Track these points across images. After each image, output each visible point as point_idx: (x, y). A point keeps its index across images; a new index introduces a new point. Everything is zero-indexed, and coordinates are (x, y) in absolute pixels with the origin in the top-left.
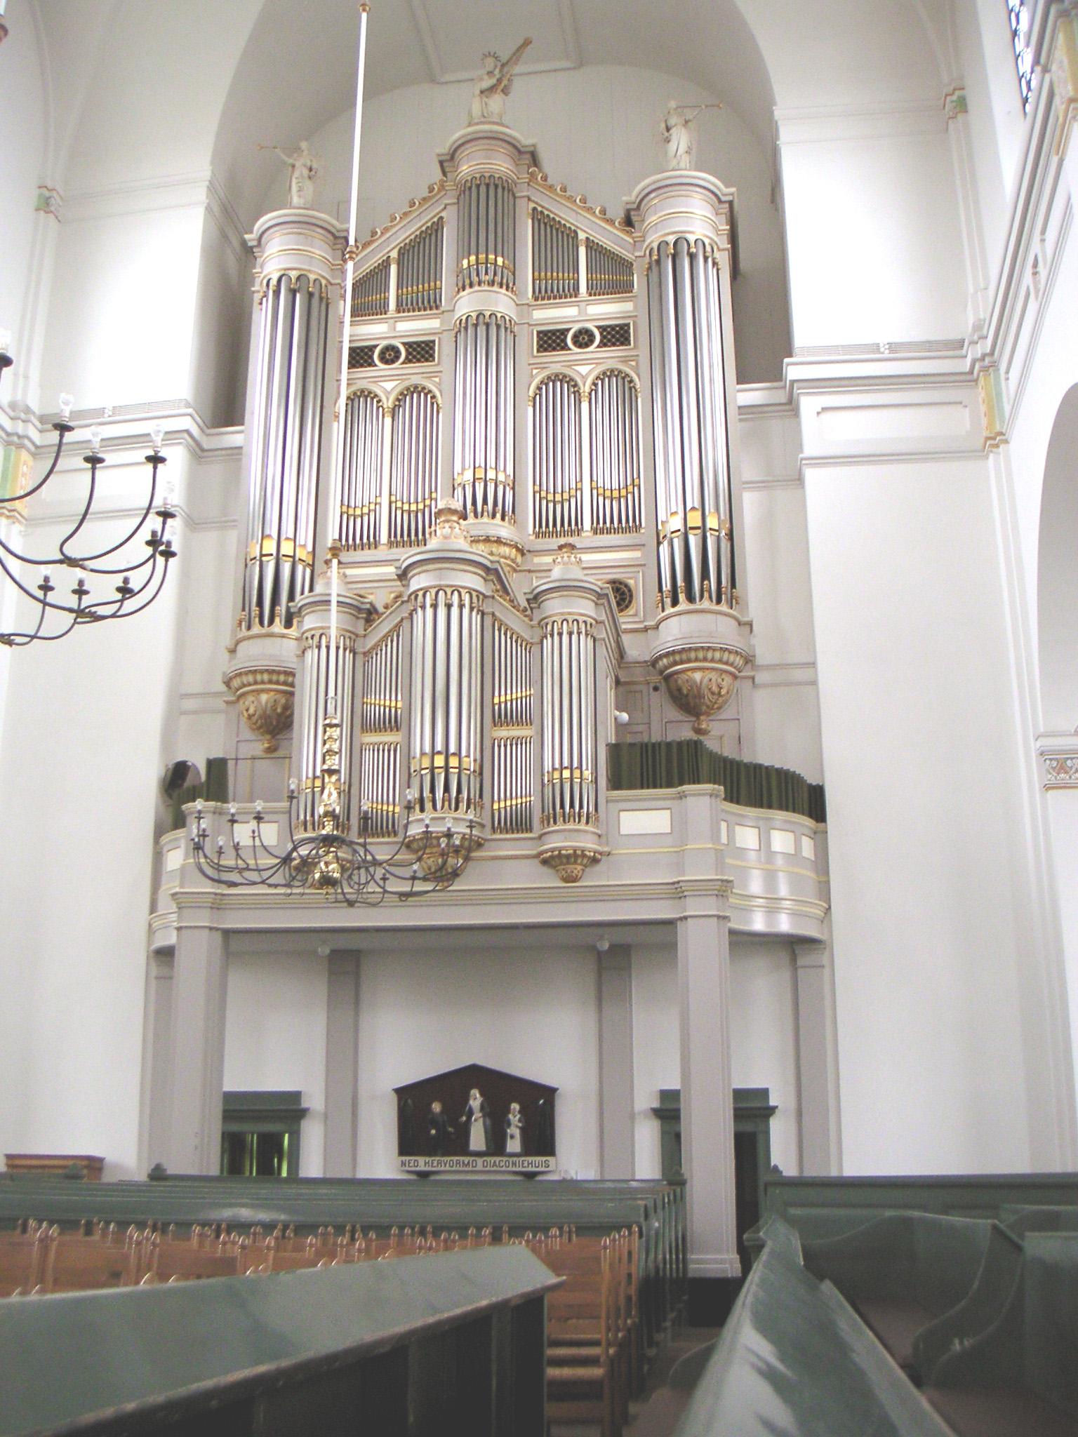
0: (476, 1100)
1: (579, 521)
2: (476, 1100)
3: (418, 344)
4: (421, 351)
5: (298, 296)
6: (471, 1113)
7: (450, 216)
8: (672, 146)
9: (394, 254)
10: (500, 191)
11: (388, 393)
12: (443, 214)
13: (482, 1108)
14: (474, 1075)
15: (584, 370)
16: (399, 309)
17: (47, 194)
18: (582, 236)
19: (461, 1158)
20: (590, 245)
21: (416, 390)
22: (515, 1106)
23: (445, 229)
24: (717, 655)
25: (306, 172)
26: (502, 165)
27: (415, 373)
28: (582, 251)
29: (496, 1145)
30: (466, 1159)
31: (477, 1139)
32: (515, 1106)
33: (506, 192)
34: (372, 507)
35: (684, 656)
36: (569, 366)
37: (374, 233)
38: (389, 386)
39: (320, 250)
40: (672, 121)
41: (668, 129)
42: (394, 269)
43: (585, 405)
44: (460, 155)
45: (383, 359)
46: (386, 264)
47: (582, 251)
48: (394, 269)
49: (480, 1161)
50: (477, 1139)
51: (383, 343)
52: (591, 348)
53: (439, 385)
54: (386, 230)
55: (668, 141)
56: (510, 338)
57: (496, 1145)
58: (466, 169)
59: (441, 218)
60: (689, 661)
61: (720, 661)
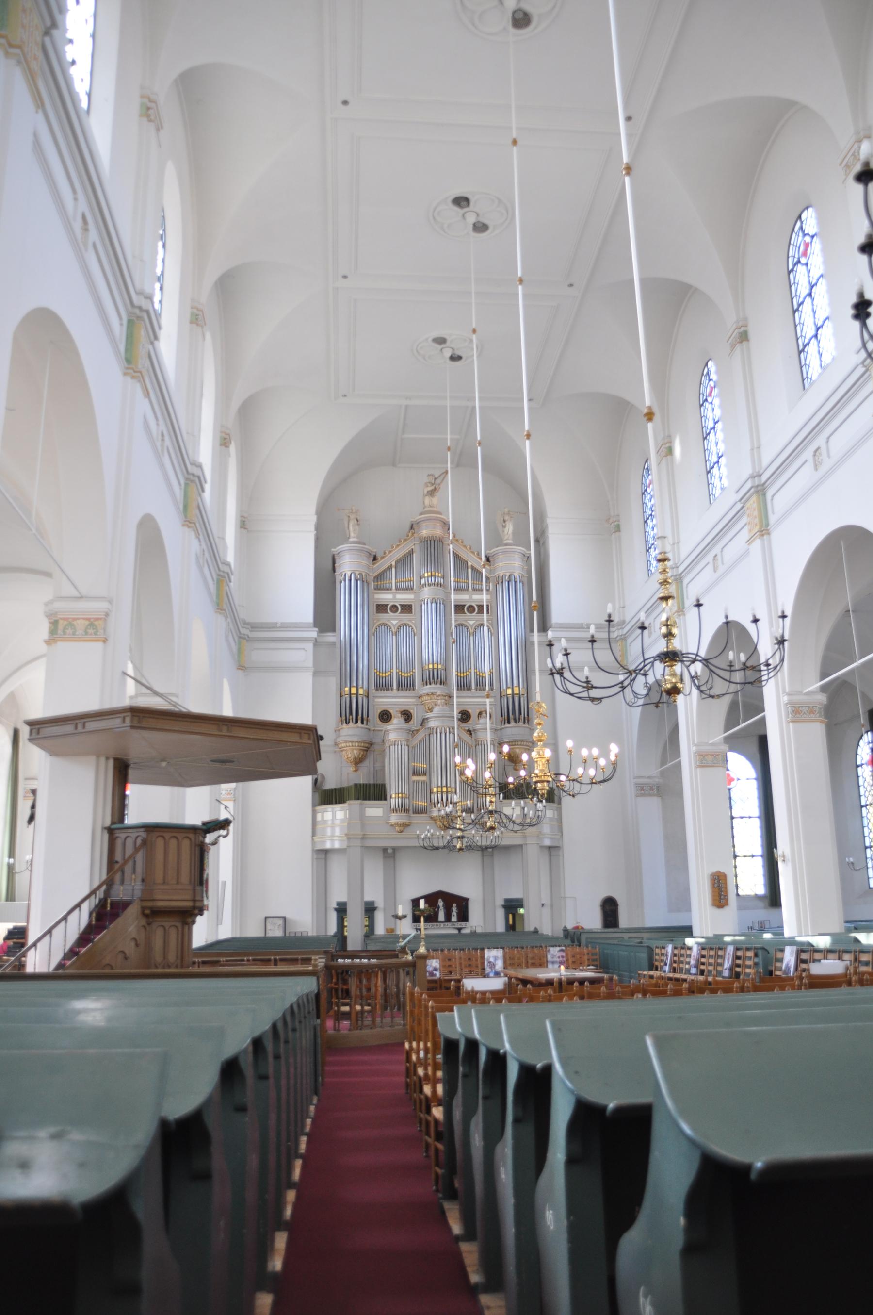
0: (441, 903)
1: (470, 686)
2: (441, 903)
3: (406, 605)
4: (407, 608)
5: (359, 582)
6: (439, 907)
7: (416, 549)
8: (506, 530)
9: (393, 563)
10: (436, 542)
11: (394, 625)
12: (413, 547)
13: (443, 906)
14: (440, 894)
15: (472, 622)
16: (397, 589)
17: (244, 519)
18: (470, 564)
19: (435, 924)
20: (473, 568)
21: (406, 625)
22: (454, 905)
23: (414, 555)
24: (525, 743)
25: (356, 522)
26: (438, 532)
27: (405, 618)
28: (470, 570)
29: (448, 919)
30: (437, 924)
31: (441, 916)
32: (454, 905)
33: (439, 542)
34: (389, 673)
35: (513, 743)
36: (466, 621)
37: (385, 553)
38: (394, 622)
39: (365, 561)
40: (506, 518)
41: (504, 521)
42: (393, 570)
43: (472, 638)
44: (424, 524)
45: (392, 611)
46: (390, 567)
47: (470, 570)
48: (393, 570)
49: (442, 924)
50: (441, 916)
51: (391, 604)
52: (474, 614)
53: (415, 624)
54: (390, 552)
55: (504, 527)
56: (442, 606)
57: (448, 919)
58: (425, 532)
59: (412, 549)
60: (515, 745)
61: (526, 746)
